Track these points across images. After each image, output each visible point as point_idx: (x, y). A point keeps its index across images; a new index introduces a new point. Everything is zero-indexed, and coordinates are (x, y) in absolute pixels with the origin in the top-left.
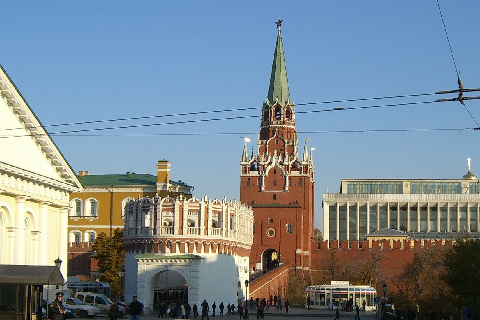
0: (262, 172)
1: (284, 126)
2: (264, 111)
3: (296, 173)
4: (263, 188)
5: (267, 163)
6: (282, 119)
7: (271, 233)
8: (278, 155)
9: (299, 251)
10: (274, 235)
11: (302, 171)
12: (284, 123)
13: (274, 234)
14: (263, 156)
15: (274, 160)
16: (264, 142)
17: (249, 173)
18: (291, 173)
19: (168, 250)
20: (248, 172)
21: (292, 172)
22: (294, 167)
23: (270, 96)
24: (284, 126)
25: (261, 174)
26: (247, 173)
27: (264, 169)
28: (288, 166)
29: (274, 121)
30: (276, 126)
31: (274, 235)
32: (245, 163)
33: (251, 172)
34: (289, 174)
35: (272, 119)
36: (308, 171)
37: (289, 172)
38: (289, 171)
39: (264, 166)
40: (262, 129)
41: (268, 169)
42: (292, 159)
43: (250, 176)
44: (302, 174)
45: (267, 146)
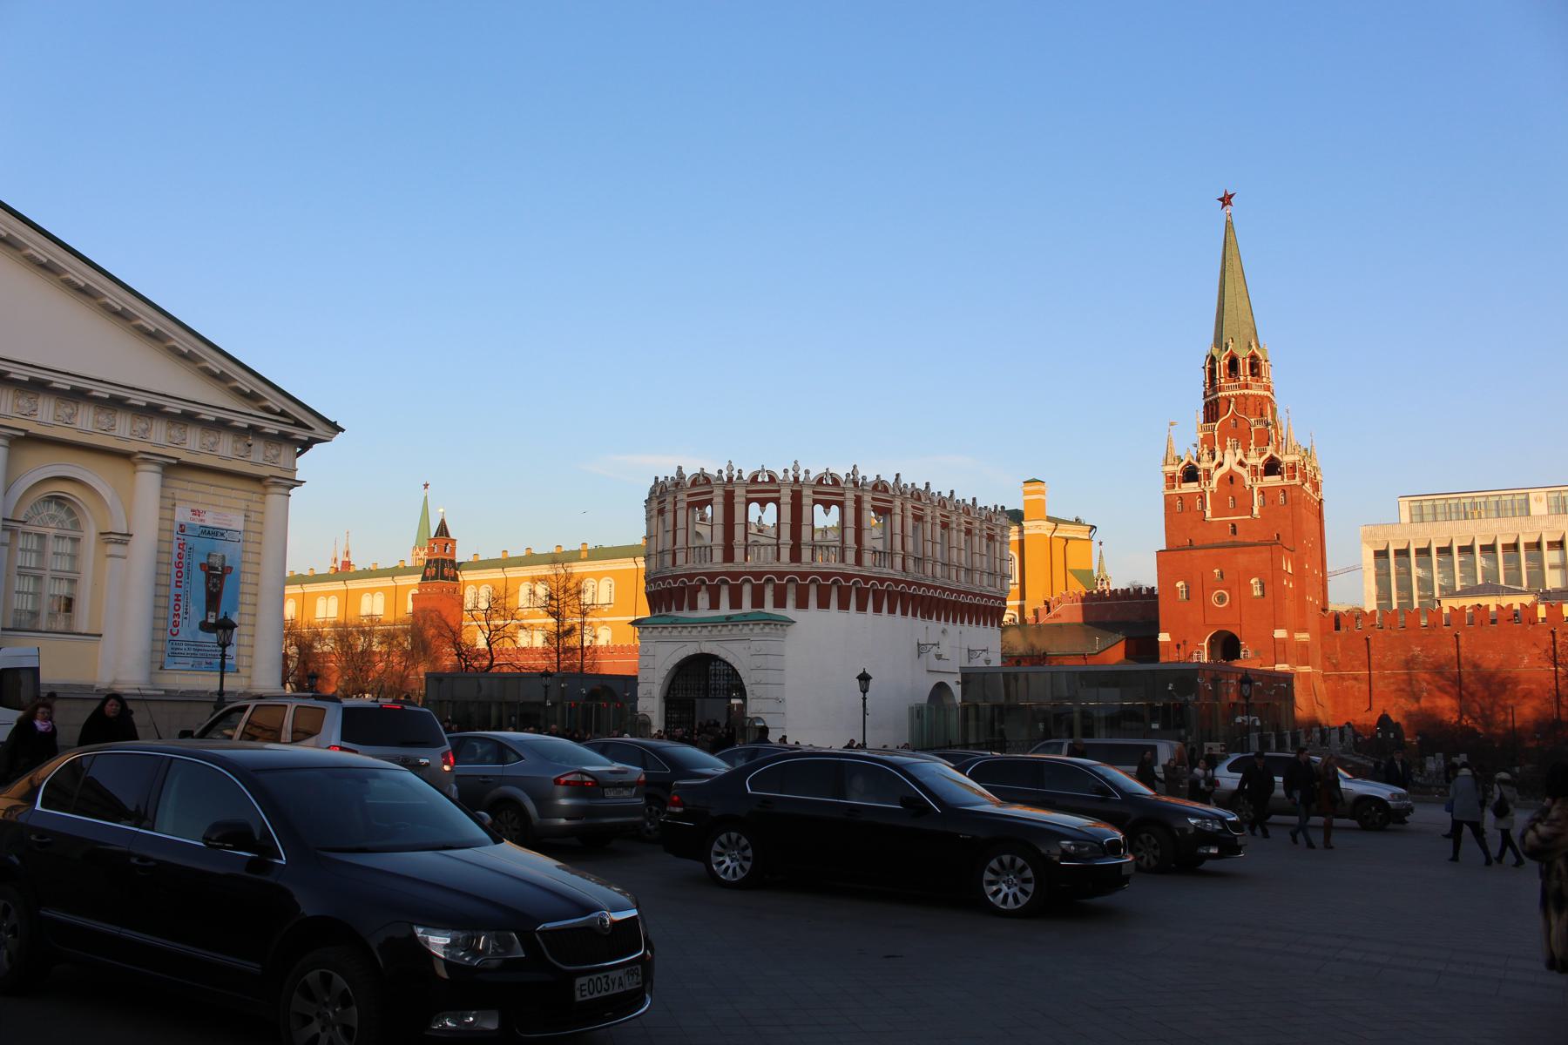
0: (1205, 483)
1: (1246, 392)
3: (1272, 481)
4: (1208, 514)
6: (1242, 378)
7: (1221, 599)
8: (1234, 448)
9: (1280, 634)
10: (1226, 603)
11: (1285, 475)
12: (1247, 386)
13: (1228, 600)
14: (1206, 451)
17: (1180, 487)
18: (1262, 480)
19: (703, 599)
20: (1177, 486)
21: (1267, 479)
22: (1272, 467)
23: (1219, 341)
24: (1246, 392)
25: (1203, 486)
26: (1177, 488)
27: (1209, 476)
28: (1256, 466)
30: (1231, 393)
31: (1226, 603)
32: (1170, 469)
33: (1183, 485)
34: (1259, 482)
35: (1222, 381)
36: (1297, 474)
37: (1259, 479)
38: (1259, 477)
39: (1208, 471)
40: (1206, 404)
41: (1217, 475)
42: (1261, 455)
44: (1285, 480)
45: (1216, 433)
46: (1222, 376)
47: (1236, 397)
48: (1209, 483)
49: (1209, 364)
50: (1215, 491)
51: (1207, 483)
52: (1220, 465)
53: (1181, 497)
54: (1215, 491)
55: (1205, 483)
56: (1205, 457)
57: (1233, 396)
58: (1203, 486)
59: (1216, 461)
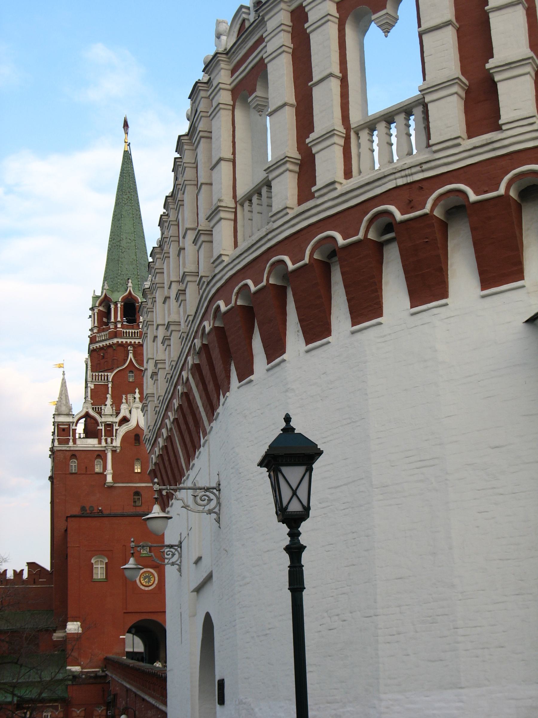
2: (96, 310)
4: (109, 479)
5: (117, 420)
15: (134, 411)
16: (104, 375)
20: (71, 441)
25: (103, 444)
26: (71, 443)
29: (125, 331)
30: (129, 341)
35: (119, 326)
41: (123, 430)
43: (77, 449)
46: (119, 319)
47: (133, 345)
48: (112, 440)
49: (100, 305)
50: (118, 451)
51: (109, 440)
52: (125, 420)
53: (74, 454)
54: (118, 451)
55: (106, 440)
56: (108, 409)
57: (130, 344)
58: (103, 444)
59: (120, 416)
